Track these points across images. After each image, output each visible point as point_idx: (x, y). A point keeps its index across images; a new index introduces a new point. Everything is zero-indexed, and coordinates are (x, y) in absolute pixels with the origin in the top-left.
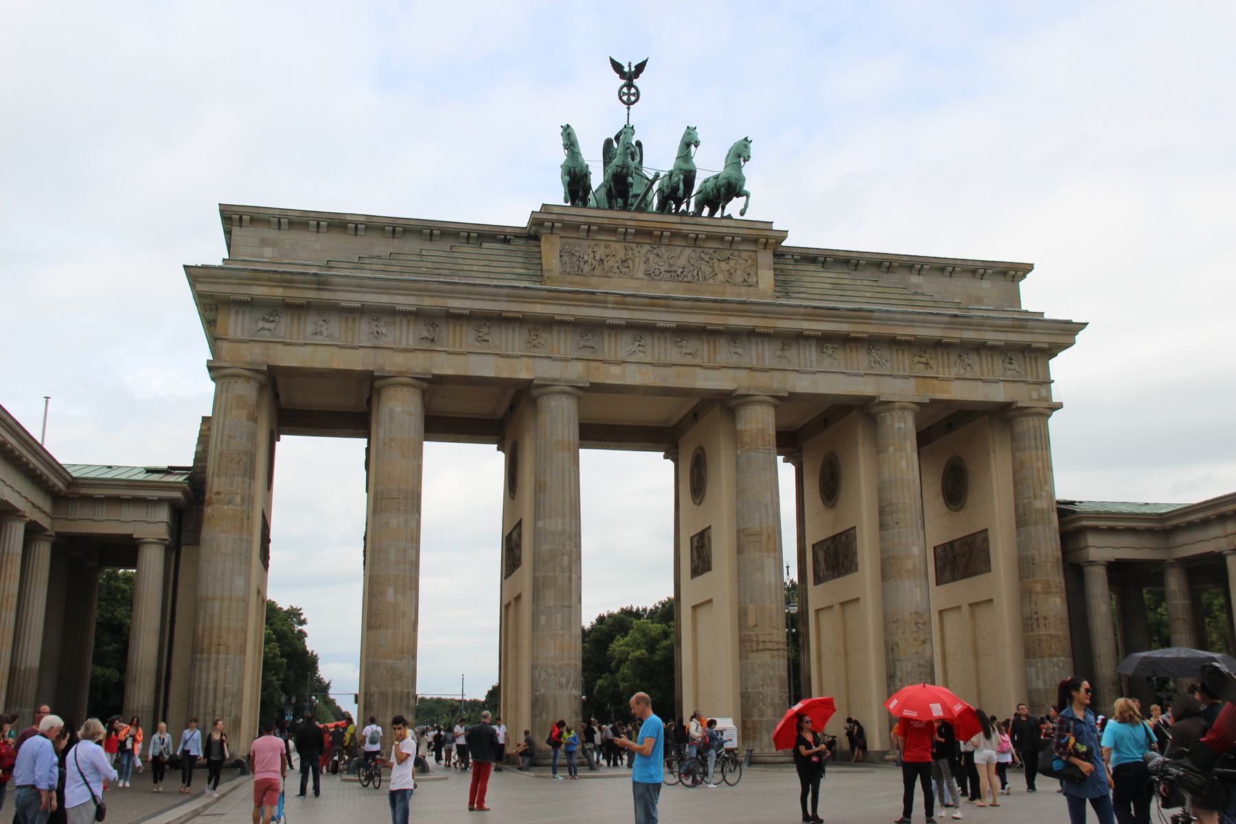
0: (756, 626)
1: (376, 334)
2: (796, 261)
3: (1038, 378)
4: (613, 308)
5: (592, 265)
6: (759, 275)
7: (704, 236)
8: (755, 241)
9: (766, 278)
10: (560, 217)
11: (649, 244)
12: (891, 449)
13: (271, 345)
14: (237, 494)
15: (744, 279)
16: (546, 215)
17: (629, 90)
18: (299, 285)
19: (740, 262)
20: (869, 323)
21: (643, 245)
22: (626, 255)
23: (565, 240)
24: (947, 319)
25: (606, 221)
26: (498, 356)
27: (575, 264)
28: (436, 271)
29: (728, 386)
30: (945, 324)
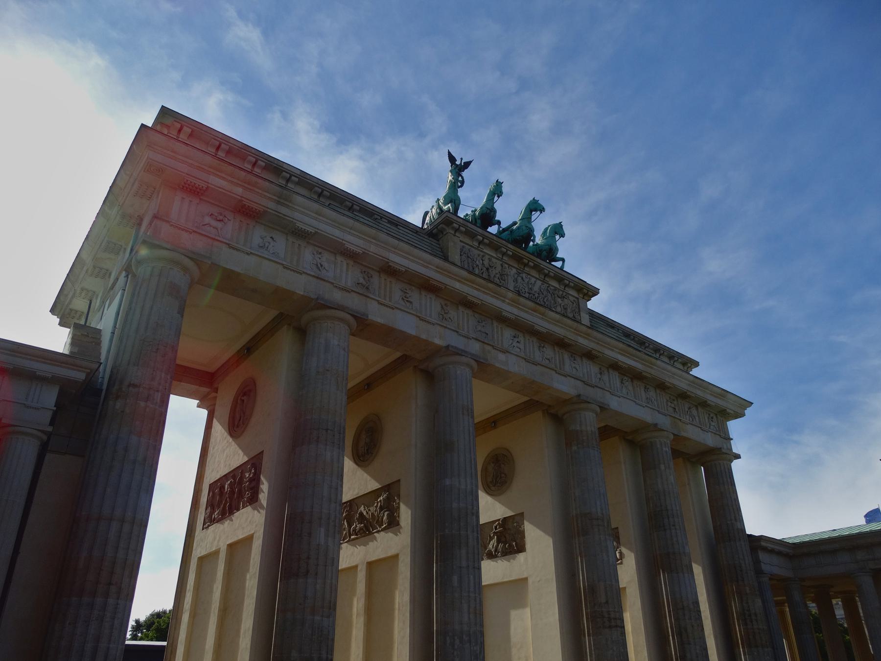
0: (607, 602)
1: (319, 265)
3: (725, 435)
4: (509, 304)
6: (581, 315)
9: (585, 319)
11: (517, 269)
12: (662, 467)
13: (216, 243)
14: (158, 391)
15: (574, 315)
18: (260, 192)
20: (652, 368)
26: (418, 319)
29: (573, 392)
30: (689, 381)
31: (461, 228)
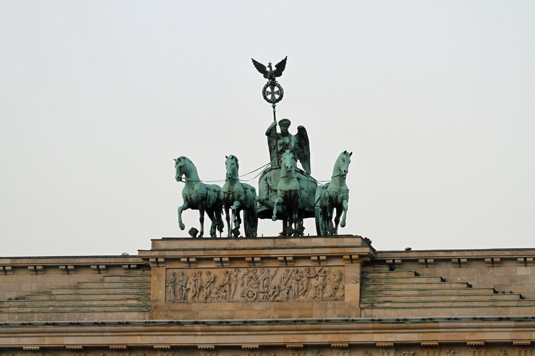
2: (398, 264)
5: (193, 292)
7: (291, 258)
8: (340, 257)
10: (162, 253)
15: (332, 294)
16: (149, 252)
17: (272, 89)
19: (327, 278)
20: (438, 332)
21: (241, 269)
22: (224, 280)
23: (170, 271)
24: (512, 324)
25: (201, 253)
27: (179, 292)
28: (61, 309)
31: (159, 260)
